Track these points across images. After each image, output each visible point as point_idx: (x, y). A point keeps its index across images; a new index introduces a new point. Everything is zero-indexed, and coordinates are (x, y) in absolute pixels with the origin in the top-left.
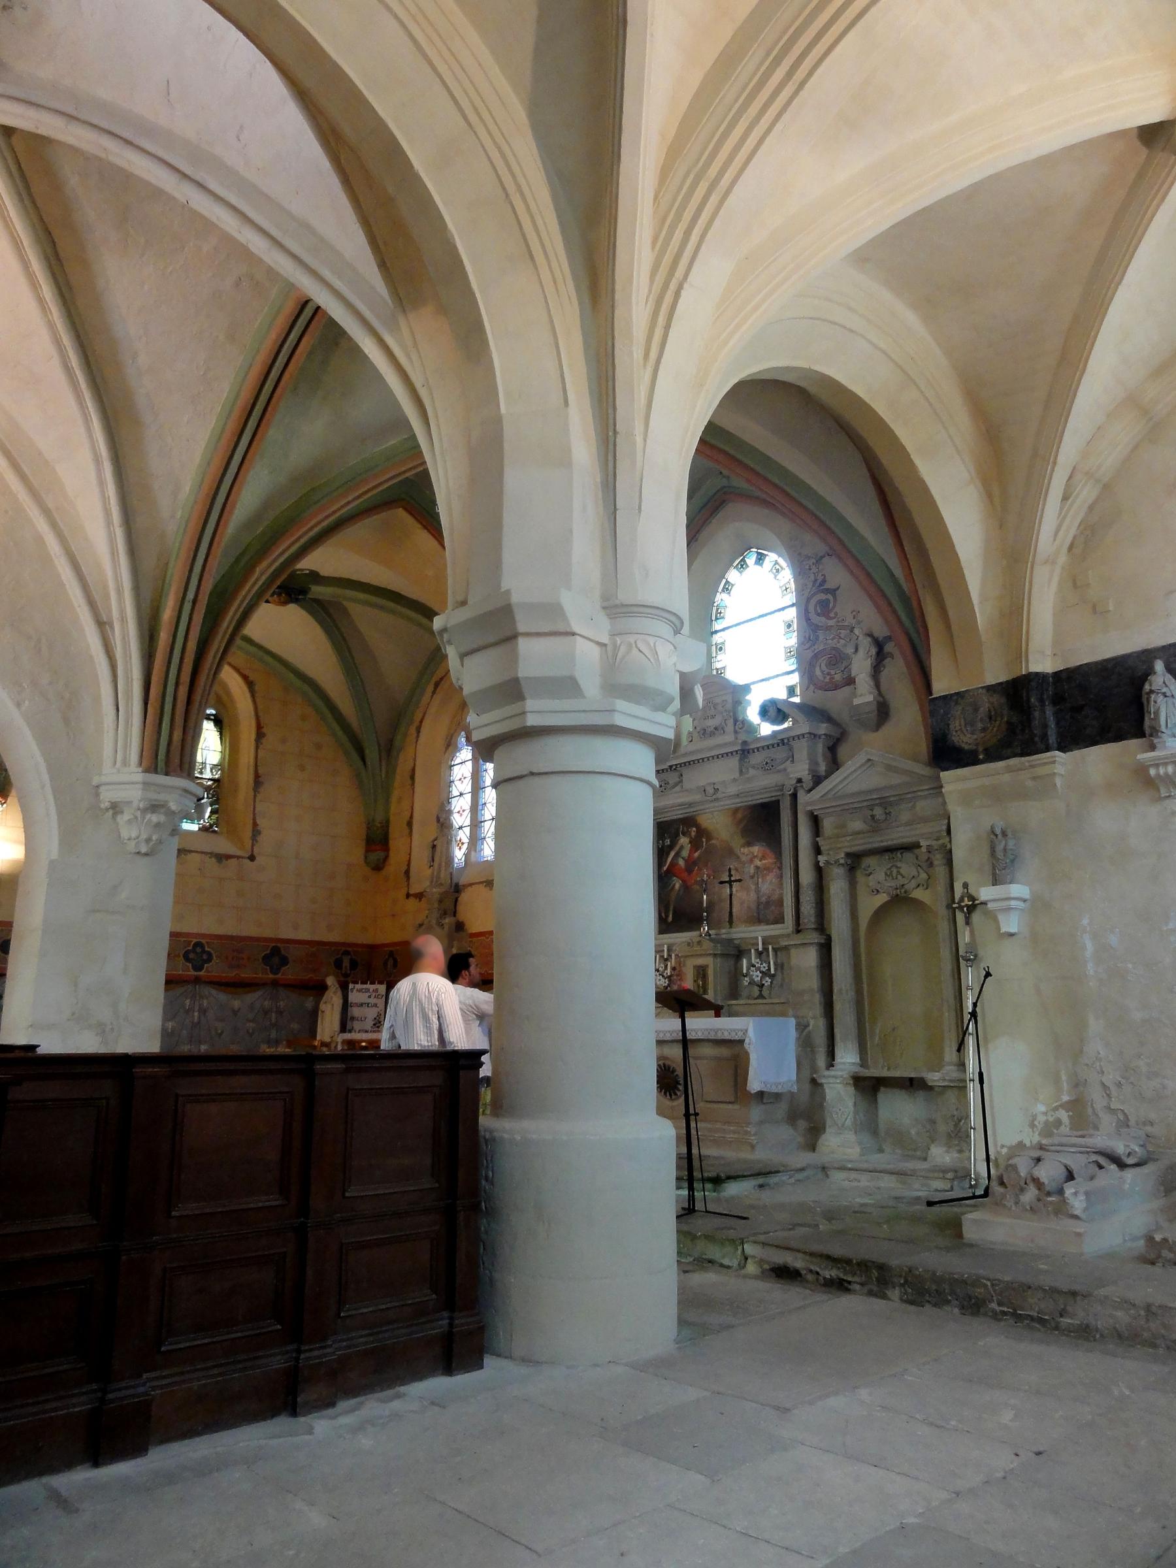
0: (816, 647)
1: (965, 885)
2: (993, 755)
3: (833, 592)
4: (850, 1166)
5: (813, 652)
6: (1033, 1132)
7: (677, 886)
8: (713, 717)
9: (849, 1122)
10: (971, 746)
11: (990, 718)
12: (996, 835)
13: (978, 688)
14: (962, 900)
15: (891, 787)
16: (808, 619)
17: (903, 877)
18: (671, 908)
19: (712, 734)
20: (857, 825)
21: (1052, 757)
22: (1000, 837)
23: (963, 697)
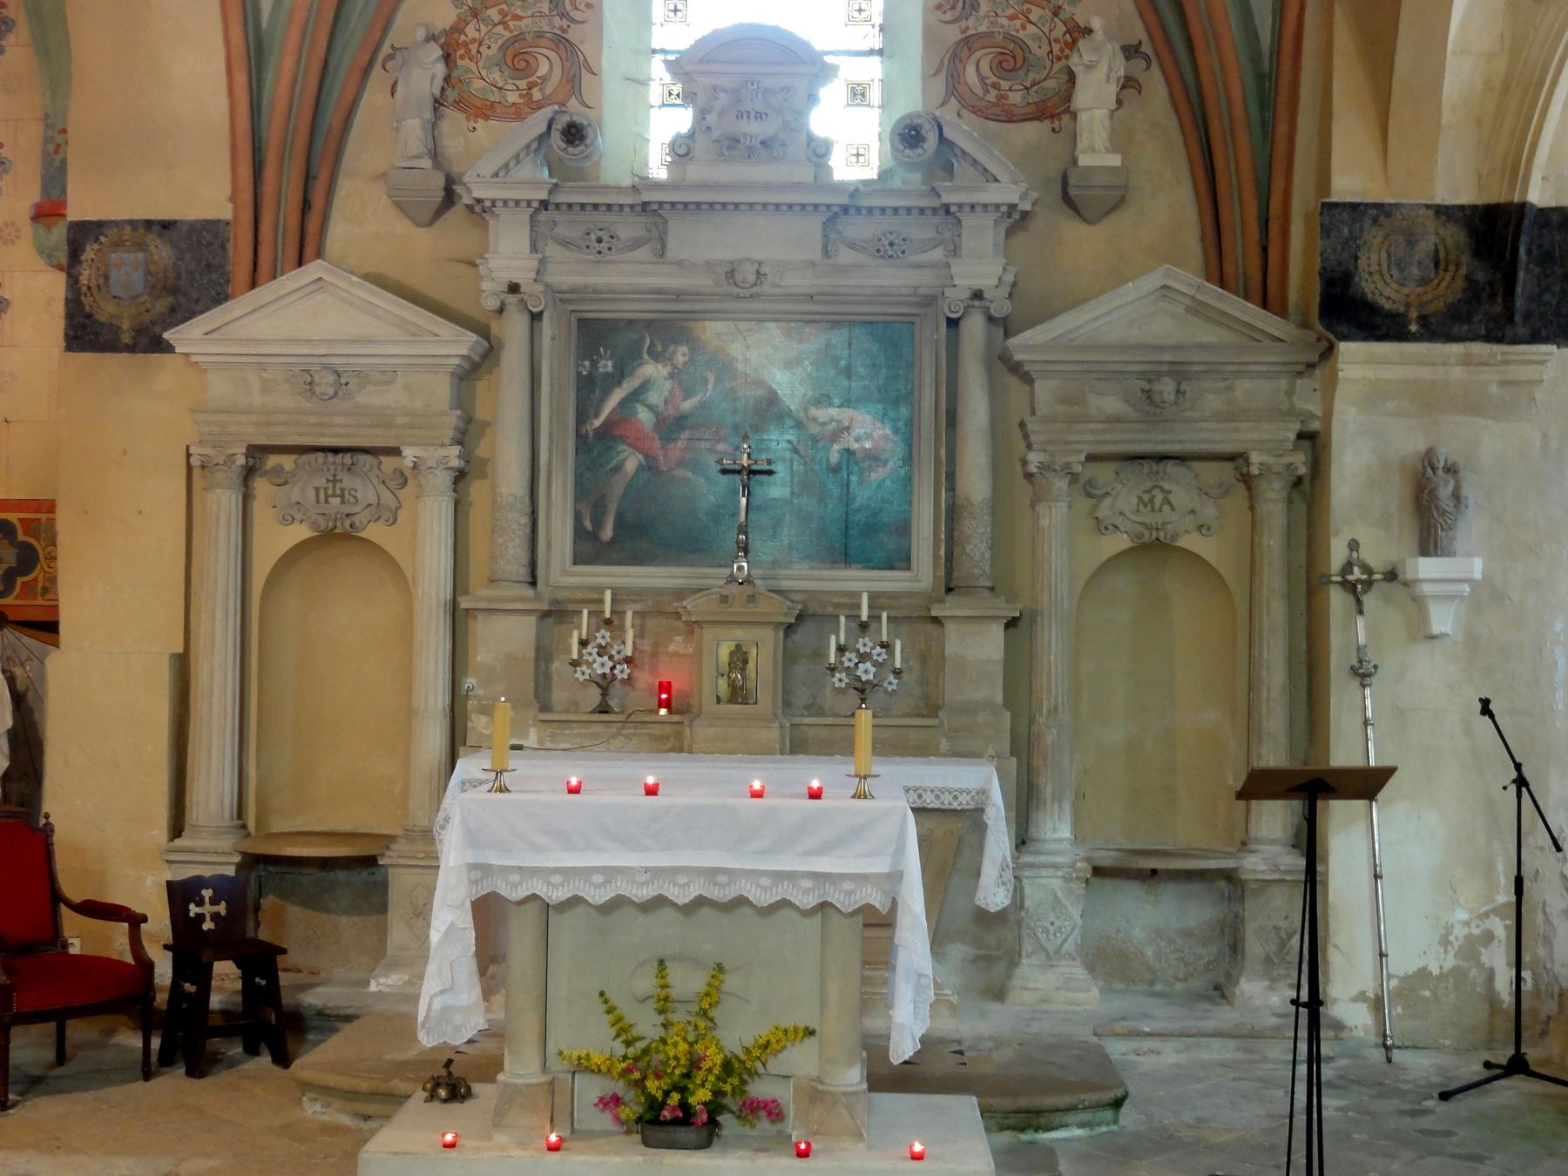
0: (971, 22)
1: (1354, 545)
2: (1438, 328)
4: (1147, 1029)
5: (963, 32)
6: (1446, 951)
7: (631, 465)
8: (760, 116)
9: (1069, 946)
10: (1395, 306)
11: (1437, 264)
12: (1434, 469)
13: (1418, 205)
14: (1348, 567)
15: (1202, 347)
17: (1173, 509)
18: (612, 508)
19: (750, 153)
20: (1111, 404)
21: (1544, 354)
22: (1440, 472)
23: (1388, 215)
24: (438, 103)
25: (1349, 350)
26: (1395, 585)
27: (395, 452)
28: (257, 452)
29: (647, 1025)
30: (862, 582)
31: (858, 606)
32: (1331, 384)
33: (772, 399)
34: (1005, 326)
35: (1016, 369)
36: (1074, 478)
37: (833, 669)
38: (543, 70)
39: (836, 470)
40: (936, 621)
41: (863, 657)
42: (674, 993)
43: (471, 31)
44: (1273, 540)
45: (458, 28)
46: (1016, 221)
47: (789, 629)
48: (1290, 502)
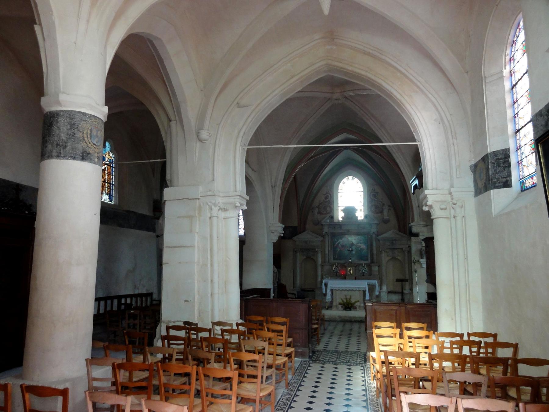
1: (414, 258)
3: (377, 193)
14: (413, 261)
26: (418, 262)
27: (315, 249)
29: (345, 301)
30: (363, 262)
32: (411, 241)
34: (378, 235)
35: (379, 240)
36: (385, 251)
37: (360, 271)
39: (359, 250)
40: (371, 266)
42: (347, 298)
44: (406, 257)
45: (319, 205)
46: (378, 225)
47: (355, 267)
48: (408, 253)
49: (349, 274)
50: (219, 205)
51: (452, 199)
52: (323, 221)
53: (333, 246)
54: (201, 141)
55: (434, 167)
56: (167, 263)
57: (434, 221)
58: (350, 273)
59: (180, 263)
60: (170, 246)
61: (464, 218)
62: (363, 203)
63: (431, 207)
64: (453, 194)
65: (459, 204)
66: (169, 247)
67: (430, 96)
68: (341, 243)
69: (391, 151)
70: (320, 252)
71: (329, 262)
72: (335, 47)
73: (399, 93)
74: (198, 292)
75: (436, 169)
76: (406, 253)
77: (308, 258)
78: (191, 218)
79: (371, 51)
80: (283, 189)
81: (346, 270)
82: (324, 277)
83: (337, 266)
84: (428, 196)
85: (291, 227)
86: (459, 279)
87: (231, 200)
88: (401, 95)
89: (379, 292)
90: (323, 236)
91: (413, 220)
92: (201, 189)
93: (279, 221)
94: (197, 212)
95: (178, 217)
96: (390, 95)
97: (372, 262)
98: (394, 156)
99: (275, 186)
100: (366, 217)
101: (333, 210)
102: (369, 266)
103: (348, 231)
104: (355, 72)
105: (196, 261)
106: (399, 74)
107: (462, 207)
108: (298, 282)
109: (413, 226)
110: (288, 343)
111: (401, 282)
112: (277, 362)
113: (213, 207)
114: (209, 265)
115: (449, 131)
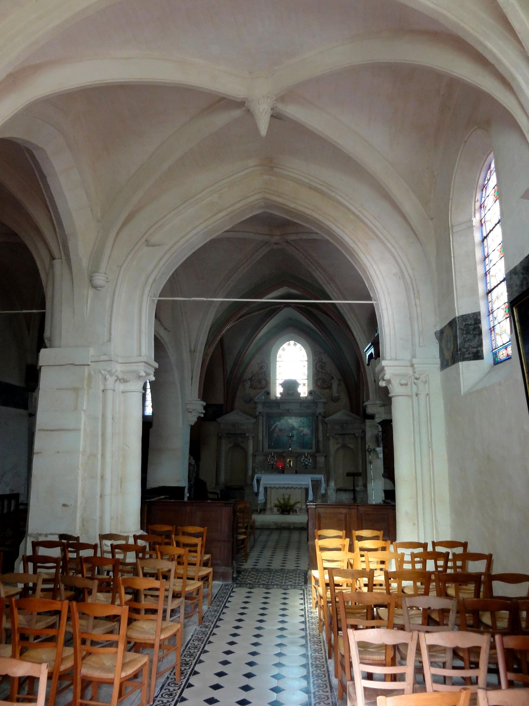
1: (369, 446)
3: (324, 363)
14: (368, 449)
16: (316, 368)
20: (337, 427)
24: (249, 387)
25: (367, 421)
27: (245, 434)
28: (227, 434)
29: (282, 502)
30: (306, 451)
31: (305, 454)
32: (365, 425)
33: (294, 427)
34: (325, 417)
35: (326, 423)
36: (333, 437)
37: (302, 463)
38: (263, 383)
41: (306, 461)
43: (253, 378)
46: (325, 403)
47: (296, 458)
48: (362, 440)
49: (288, 466)
50: (117, 374)
51: (414, 372)
52: (256, 398)
53: (269, 429)
54: (95, 287)
55: (392, 332)
56: (40, 453)
57: (393, 400)
58: (290, 465)
59: (58, 452)
60: (45, 428)
61: (427, 396)
62: (307, 375)
63: (389, 382)
64: (415, 366)
65: (423, 378)
66: (43, 430)
67: (389, 245)
68: (278, 427)
69: (342, 312)
70: (252, 438)
71: (263, 451)
72: (274, 178)
73: (351, 239)
74: (83, 493)
75: (395, 334)
76: (359, 440)
77: (237, 446)
78: (76, 390)
79: (319, 186)
80: (205, 354)
81: (285, 462)
82: (256, 470)
83: (273, 457)
84: (385, 368)
85: (215, 405)
86: (422, 474)
87: (134, 367)
88: (354, 242)
89: (326, 490)
90: (256, 417)
91: (368, 398)
92: (92, 351)
93: (199, 397)
94: (86, 383)
95: (58, 389)
96: (341, 242)
97: (318, 451)
98: (346, 317)
99: (194, 351)
100: (310, 393)
101: (270, 383)
102: (314, 456)
103: (288, 410)
104: (298, 210)
105: (81, 450)
106: (352, 216)
107: (426, 382)
108: (222, 478)
109: (368, 406)
110: (204, 562)
111: (352, 477)
112: (187, 589)
113: (108, 376)
114: (99, 456)
115: (411, 288)
